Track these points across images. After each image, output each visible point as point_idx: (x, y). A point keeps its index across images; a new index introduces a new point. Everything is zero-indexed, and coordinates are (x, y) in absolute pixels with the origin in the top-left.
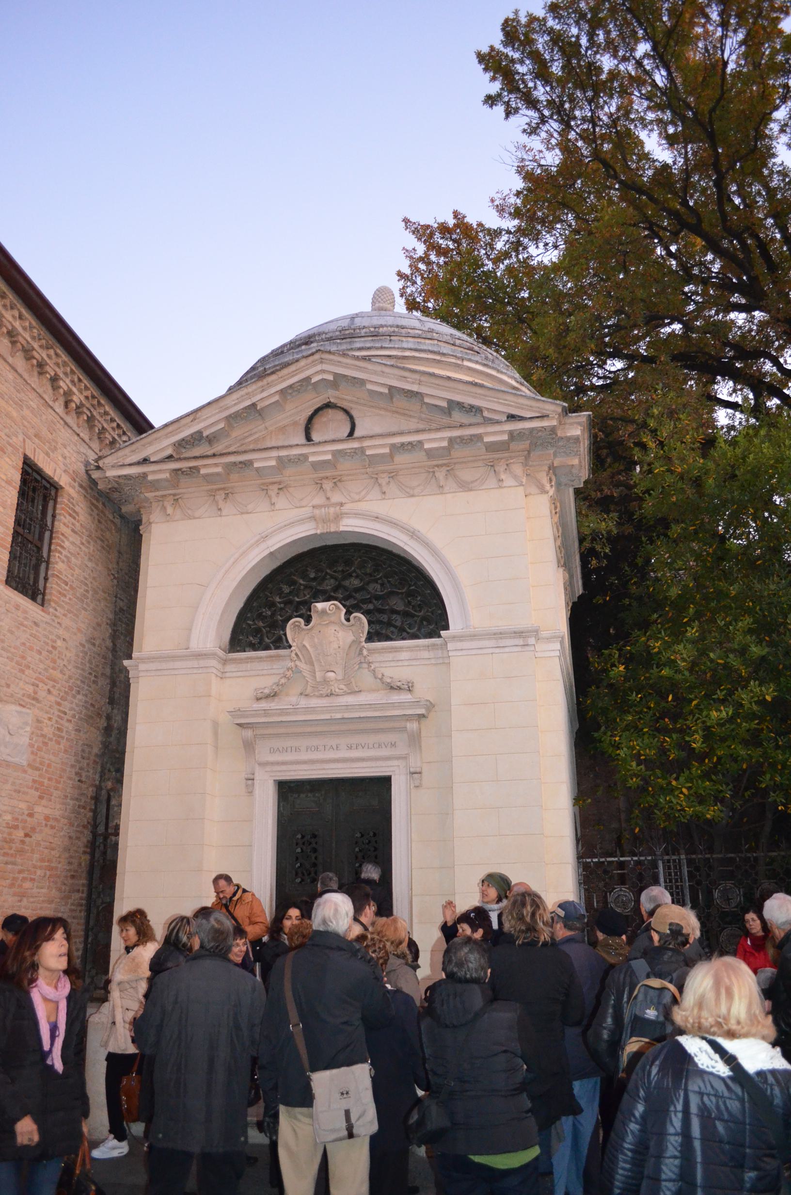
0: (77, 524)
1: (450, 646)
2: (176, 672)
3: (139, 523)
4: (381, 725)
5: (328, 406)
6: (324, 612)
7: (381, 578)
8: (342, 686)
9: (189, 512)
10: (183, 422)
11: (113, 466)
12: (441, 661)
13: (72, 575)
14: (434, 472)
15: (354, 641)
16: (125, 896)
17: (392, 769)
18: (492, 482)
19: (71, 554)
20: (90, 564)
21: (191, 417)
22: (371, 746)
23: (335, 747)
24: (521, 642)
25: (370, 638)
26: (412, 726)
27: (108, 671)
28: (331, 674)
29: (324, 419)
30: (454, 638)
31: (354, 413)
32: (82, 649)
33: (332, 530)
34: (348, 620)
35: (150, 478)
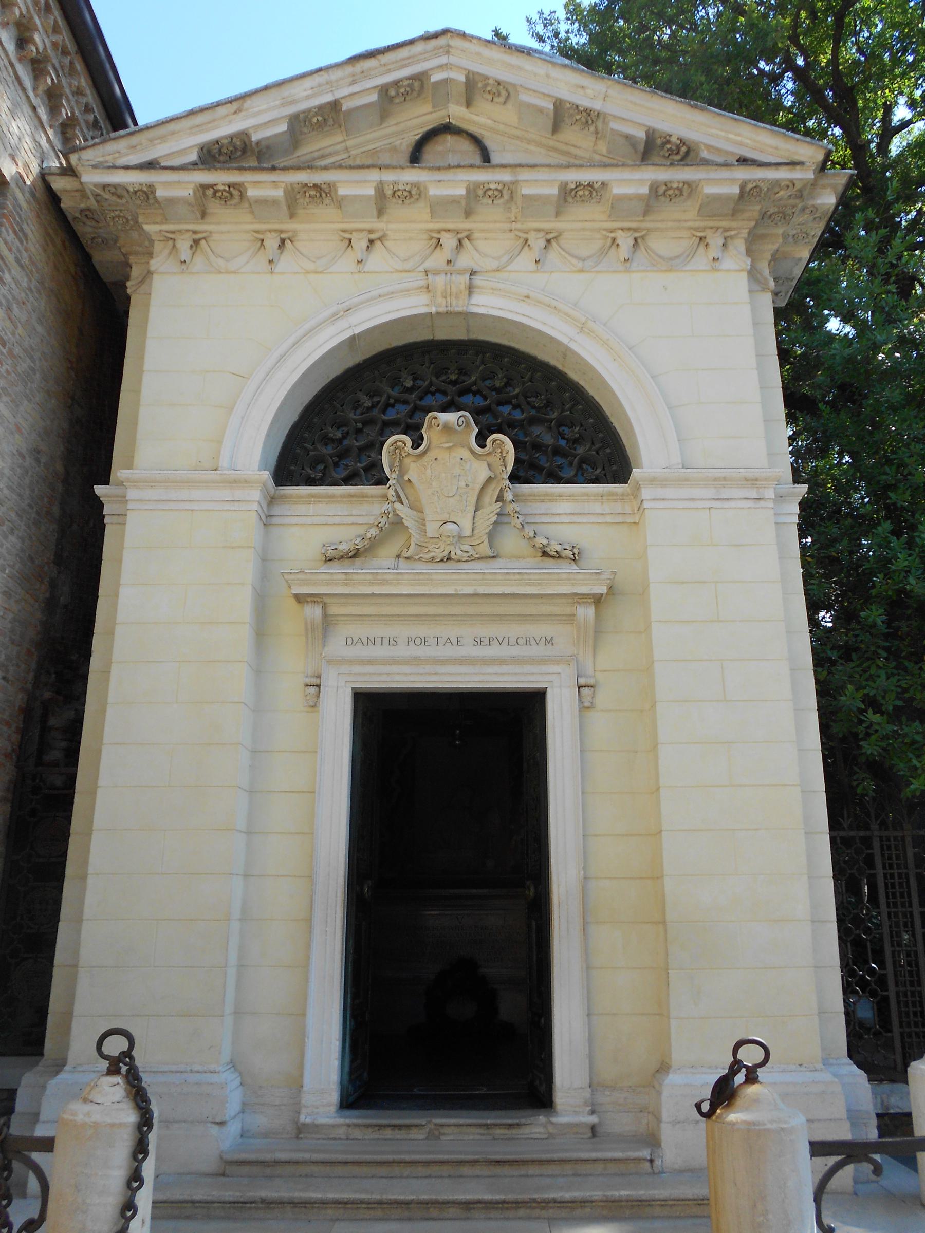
0: (25, 254)
1: (646, 493)
2: (195, 506)
3: (122, 285)
4: (531, 609)
6: (447, 428)
7: (516, 396)
8: (466, 547)
9: (220, 262)
10: (221, 111)
11: (95, 167)
12: (620, 519)
13: (13, 334)
14: (614, 240)
15: (490, 480)
16: (91, 870)
17: (547, 678)
18: (701, 260)
19: (14, 298)
20: (40, 329)
21: (235, 106)
22: (513, 641)
23: (454, 641)
24: (753, 494)
25: (515, 478)
26: (587, 613)
27: (56, 510)
29: (439, 148)
30: (653, 481)
32: (21, 461)
34: (483, 446)
35: (160, 193)
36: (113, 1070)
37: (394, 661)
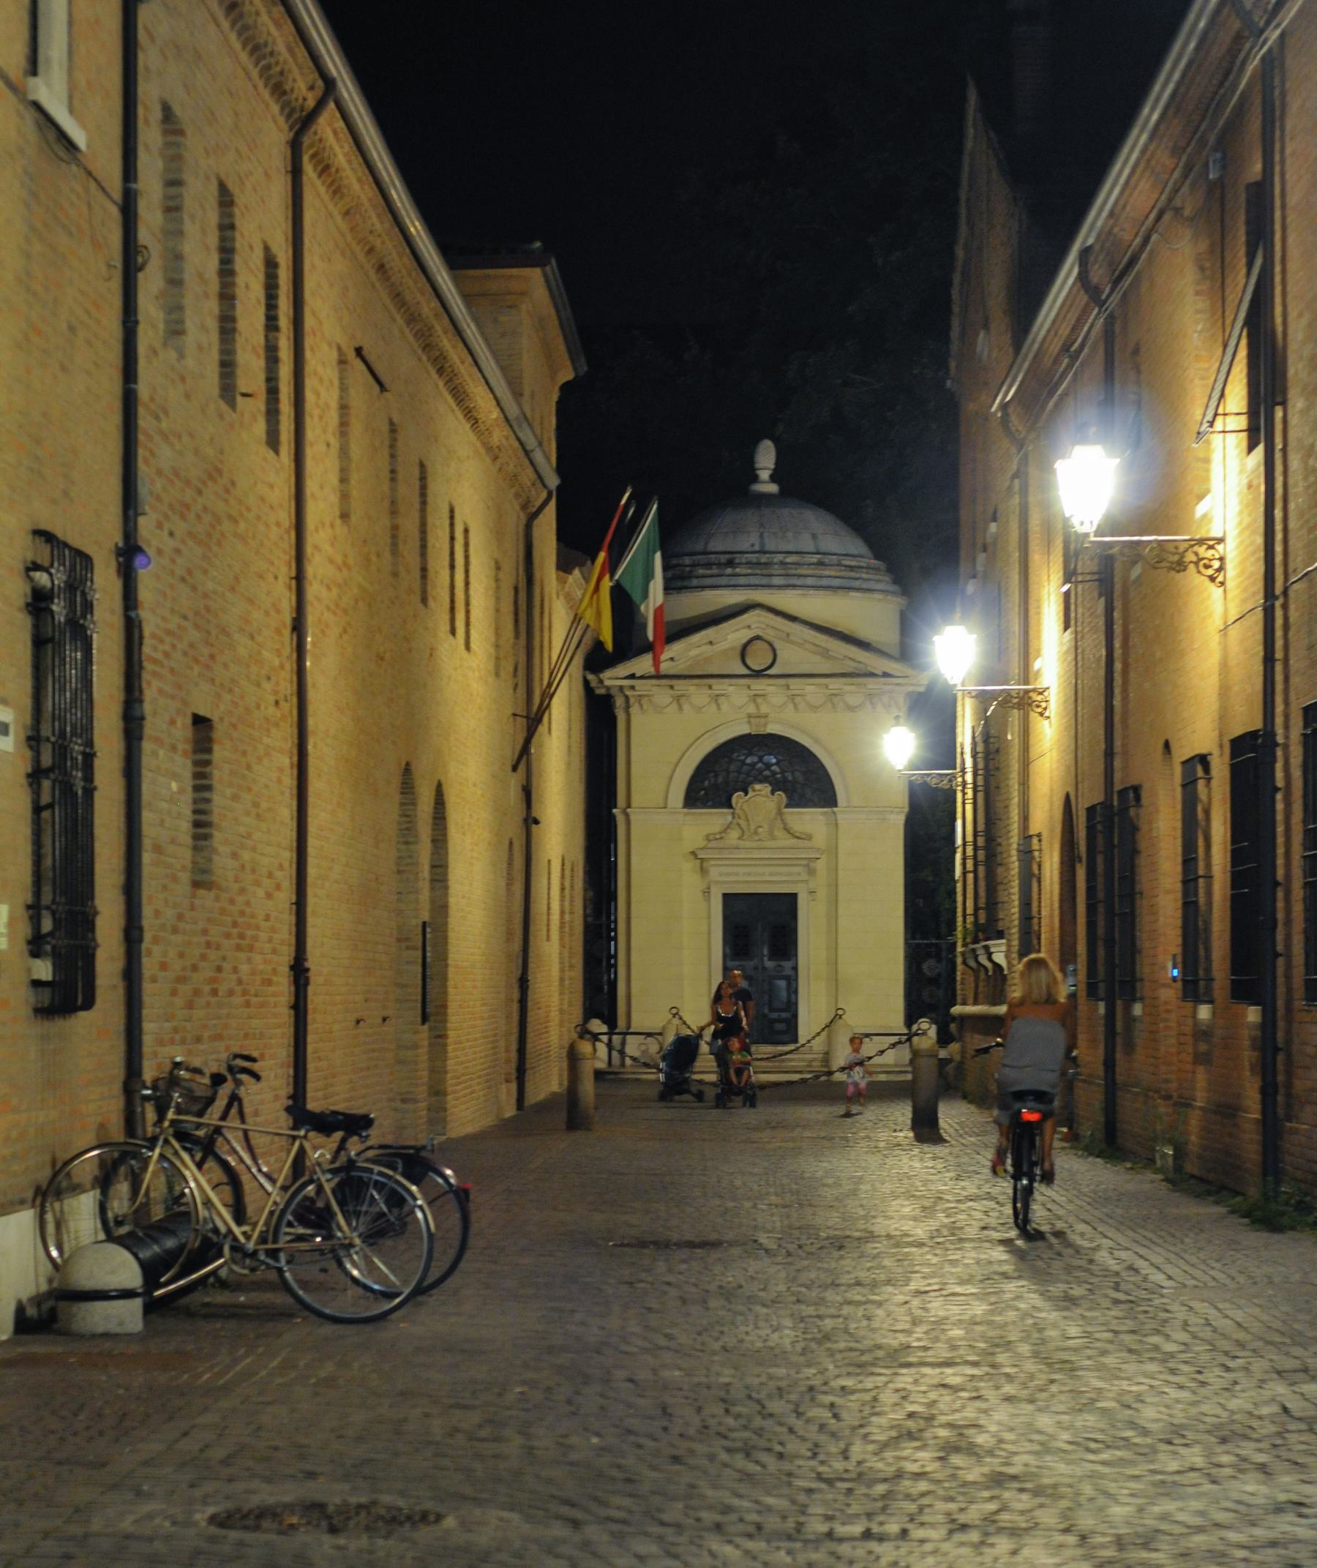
1: (839, 816)
5: (758, 638)
31: (777, 646)
33: (762, 731)
36: (674, 1015)
37: (738, 882)
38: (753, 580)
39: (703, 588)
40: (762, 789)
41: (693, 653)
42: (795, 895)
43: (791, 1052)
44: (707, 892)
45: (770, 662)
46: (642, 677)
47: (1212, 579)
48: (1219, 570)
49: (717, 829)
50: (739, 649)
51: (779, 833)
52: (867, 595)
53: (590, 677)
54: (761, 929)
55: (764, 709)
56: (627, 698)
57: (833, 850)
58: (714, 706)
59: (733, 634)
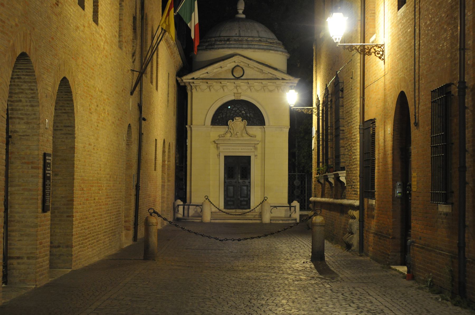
5: (238, 66)
28: (238, 134)
33: (239, 99)
37: (230, 152)
38: (236, 46)
39: (219, 48)
40: (239, 119)
41: (215, 71)
42: (250, 157)
43: (248, 212)
44: (219, 155)
45: (242, 74)
46: (197, 79)
47: (380, 58)
48: (382, 55)
49: (222, 133)
50: (231, 69)
51: (245, 135)
52: (276, 52)
53: (178, 79)
54: (238, 170)
55: (240, 91)
56: (191, 86)
57: (264, 141)
58: (222, 90)
59: (229, 64)
